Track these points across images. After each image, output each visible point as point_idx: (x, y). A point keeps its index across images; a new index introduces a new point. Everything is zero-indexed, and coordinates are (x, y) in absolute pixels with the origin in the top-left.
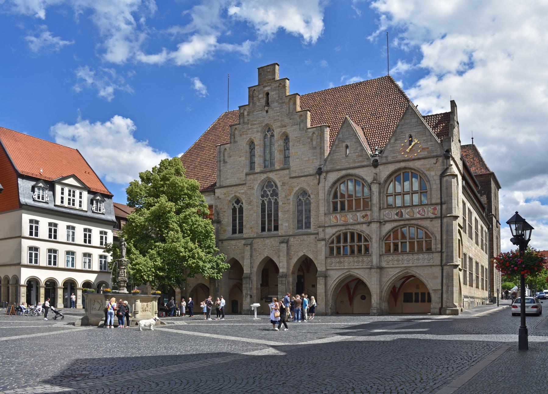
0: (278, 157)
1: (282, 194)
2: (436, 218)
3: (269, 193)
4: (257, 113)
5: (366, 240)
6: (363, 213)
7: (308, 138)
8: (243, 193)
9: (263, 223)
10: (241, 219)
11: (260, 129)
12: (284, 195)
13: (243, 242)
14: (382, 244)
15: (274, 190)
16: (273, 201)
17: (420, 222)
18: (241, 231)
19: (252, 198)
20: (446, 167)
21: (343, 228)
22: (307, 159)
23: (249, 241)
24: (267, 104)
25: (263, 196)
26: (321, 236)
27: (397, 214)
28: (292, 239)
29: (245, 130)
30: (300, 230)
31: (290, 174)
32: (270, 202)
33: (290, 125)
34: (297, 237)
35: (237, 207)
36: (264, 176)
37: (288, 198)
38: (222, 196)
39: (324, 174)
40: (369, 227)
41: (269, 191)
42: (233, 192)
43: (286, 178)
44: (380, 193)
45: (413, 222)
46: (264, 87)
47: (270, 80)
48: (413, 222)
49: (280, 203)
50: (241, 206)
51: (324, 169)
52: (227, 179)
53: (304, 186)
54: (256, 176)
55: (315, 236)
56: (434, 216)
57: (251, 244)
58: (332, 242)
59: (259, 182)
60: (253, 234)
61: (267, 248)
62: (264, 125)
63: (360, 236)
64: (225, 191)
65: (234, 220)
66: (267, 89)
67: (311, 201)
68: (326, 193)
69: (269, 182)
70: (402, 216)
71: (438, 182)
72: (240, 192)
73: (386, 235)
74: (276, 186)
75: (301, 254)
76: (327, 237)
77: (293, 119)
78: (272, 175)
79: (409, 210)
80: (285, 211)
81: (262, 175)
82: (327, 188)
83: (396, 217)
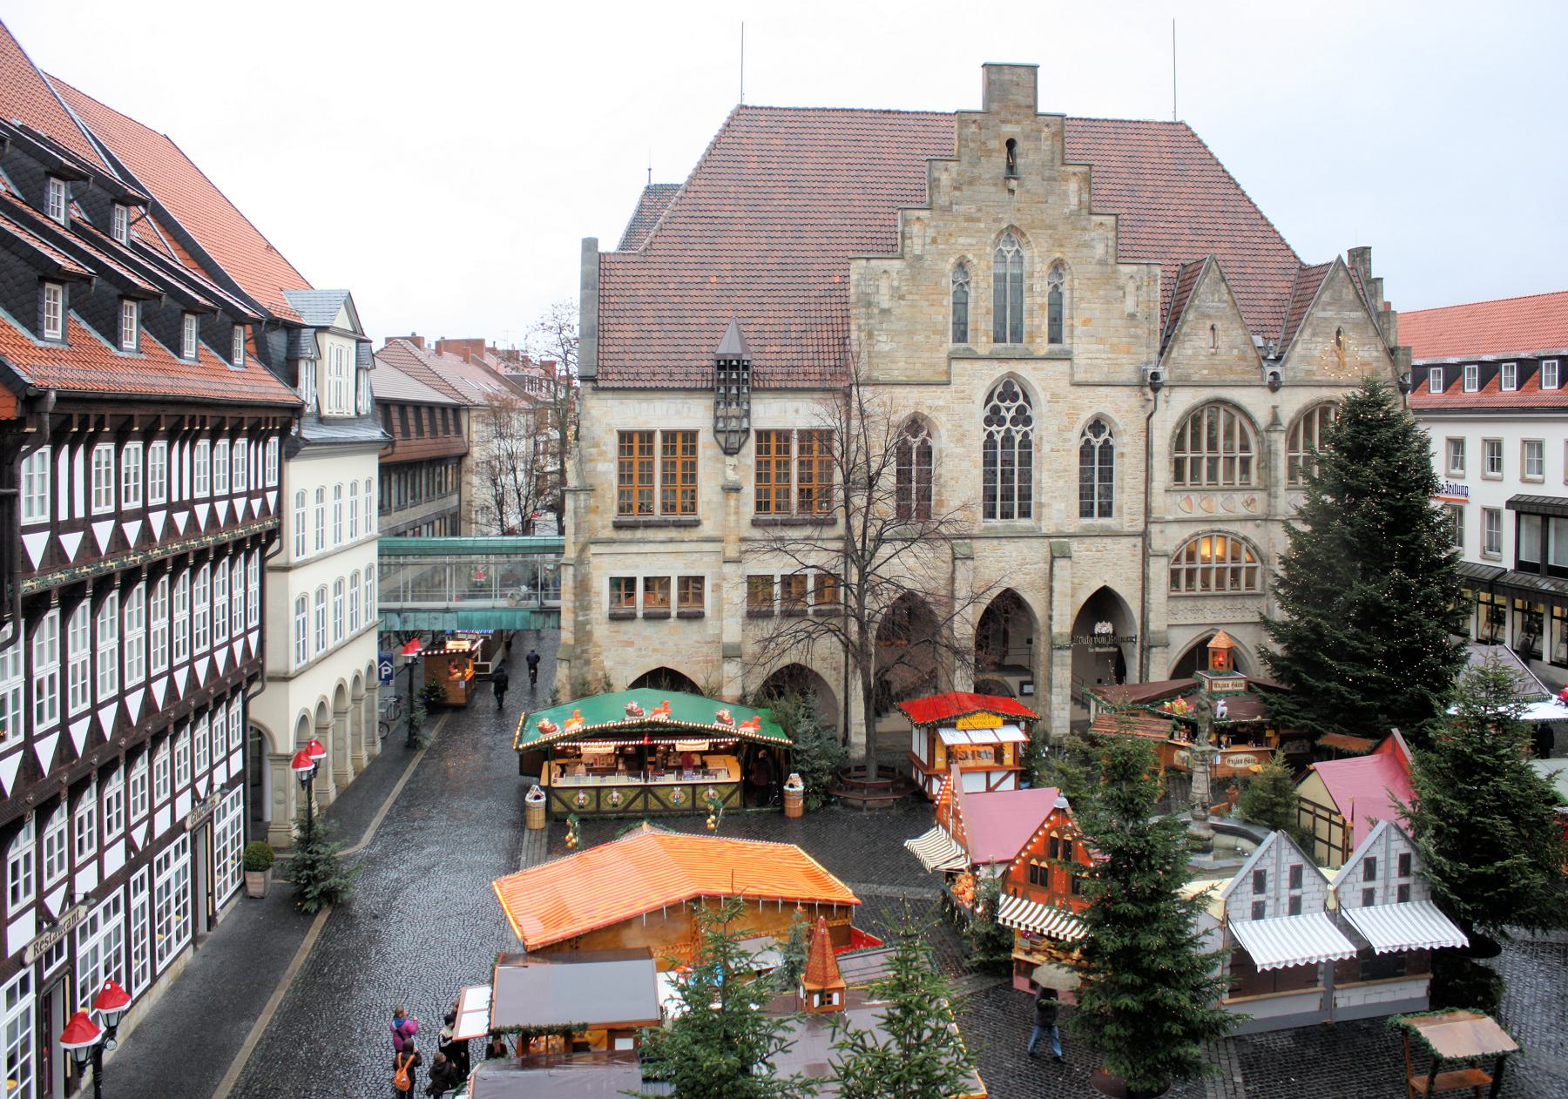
0: (1037, 322)
9: (989, 495)
10: (926, 477)
15: (1021, 410)
16: (1018, 438)
19: (966, 427)
24: (1011, 168)
28: (1075, 545)
30: (1087, 521)
31: (1072, 375)
32: (1008, 439)
34: (1088, 541)
35: (915, 443)
36: (1000, 370)
42: (906, 402)
47: (1018, 106)
51: (1165, 376)
58: (1178, 559)
61: (1007, 562)
66: (1010, 130)
75: (1096, 586)
76: (1170, 548)
78: (1024, 370)
81: (995, 363)
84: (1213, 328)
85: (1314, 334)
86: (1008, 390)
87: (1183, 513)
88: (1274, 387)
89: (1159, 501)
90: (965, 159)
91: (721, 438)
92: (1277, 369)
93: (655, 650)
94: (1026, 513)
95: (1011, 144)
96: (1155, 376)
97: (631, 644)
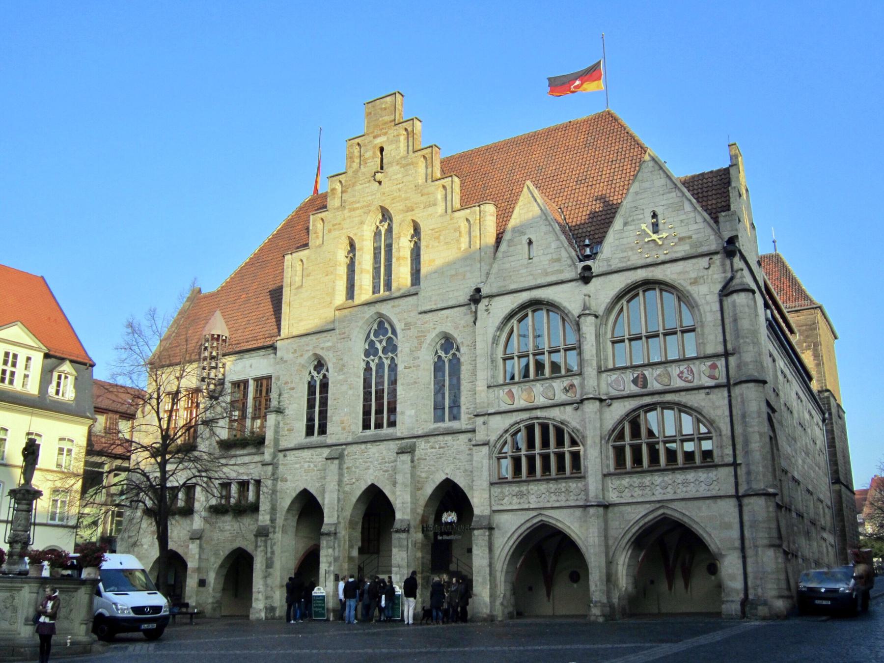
2: (717, 386)
3: (379, 347)
4: (360, 187)
5: (574, 443)
6: (566, 382)
8: (328, 349)
9: (367, 413)
10: (324, 403)
12: (408, 350)
13: (326, 452)
14: (607, 449)
16: (387, 362)
17: (683, 398)
18: (323, 431)
19: (346, 358)
20: (729, 275)
21: (525, 415)
22: (453, 272)
23: (335, 452)
25: (367, 354)
26: (480, 436)
27: (635, 381)
28: (421, 444)
29: (338, 221)
32: (380, 366)
33: (422, 206)
34: (432, 439)
37: (416, 354)
38: (289, 356)
39: (484, 302)
40: (579, 412)
41: (381, 342)
43: (412, 314)
44: (598, 336)
45: (669, 398)
46: (375, 137)
47: (386, 123)
48: (669, 398)
49: (400, 368)
50: (325, 376)
52: (301, 320)
55: (469, 435)
56: (712, 383)
57: (340, 457)
59: (360, 324)
60: (345, 435)
63: (560, 433)
64: (295, 346)
65: (311, 405)
66: (379, 141)
67: (462, 360)
68: (490, 340)
69: (381, 324)
70: (645, 385)
71: (716, 307)
72: (324, 346)
73: (613, 431)
74: (394, 332)
75: (440, 478)
76: (493, 438)
77: (428, 194)
79: (659, 370)
81: (366, 308)
82: (491, 331)
83: (634, 389)
84: (530, 242)
85: (625, 224)
94: (392, 424)
96: (478, 290)
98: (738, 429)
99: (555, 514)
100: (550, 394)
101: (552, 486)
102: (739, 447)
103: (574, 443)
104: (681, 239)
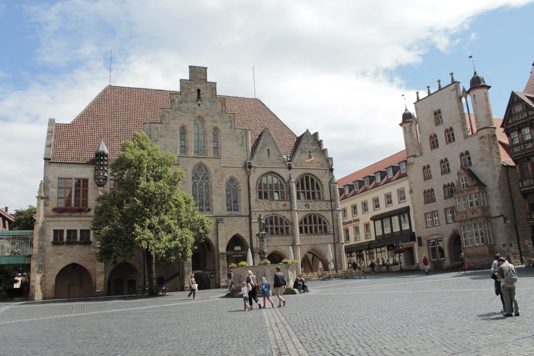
1: (214, 180)
2: (329, 210)
7: (236, 136)
11: (193, 118)
20: (331, 177)
21: (271, 213)
24: (199, 97)
25: (193, 178)
27: (306, 206)
30: (230, 212)
34: (230, 218)
36: (197, 161)
46: (196, 83)
53: (234, 175)
54: (189, 159)
56: (327, 209)
59: (193, 165)
62: (196, 115)
63: (281, 220)
66: (199, 86)
70: (309, 208)
71: (328, 185)
75: (234, 233)
80: (218, 195)
81: (195, 159)
84: (268, 150)
86: (201, 167)
87: (262, 209)
88: (290, 168)
89: (253, 204)
90: (183, 94)
91: (97, 181)
92: (290, 163)
93: (70, 257)
95: (199, 91)
97: (61, 254)
98: (335, 224)
99: (281, 248)
100: (278, 206)
101: (280, 238)
102: (335, 229)
103: (286, 224)
104: (318, 162)
